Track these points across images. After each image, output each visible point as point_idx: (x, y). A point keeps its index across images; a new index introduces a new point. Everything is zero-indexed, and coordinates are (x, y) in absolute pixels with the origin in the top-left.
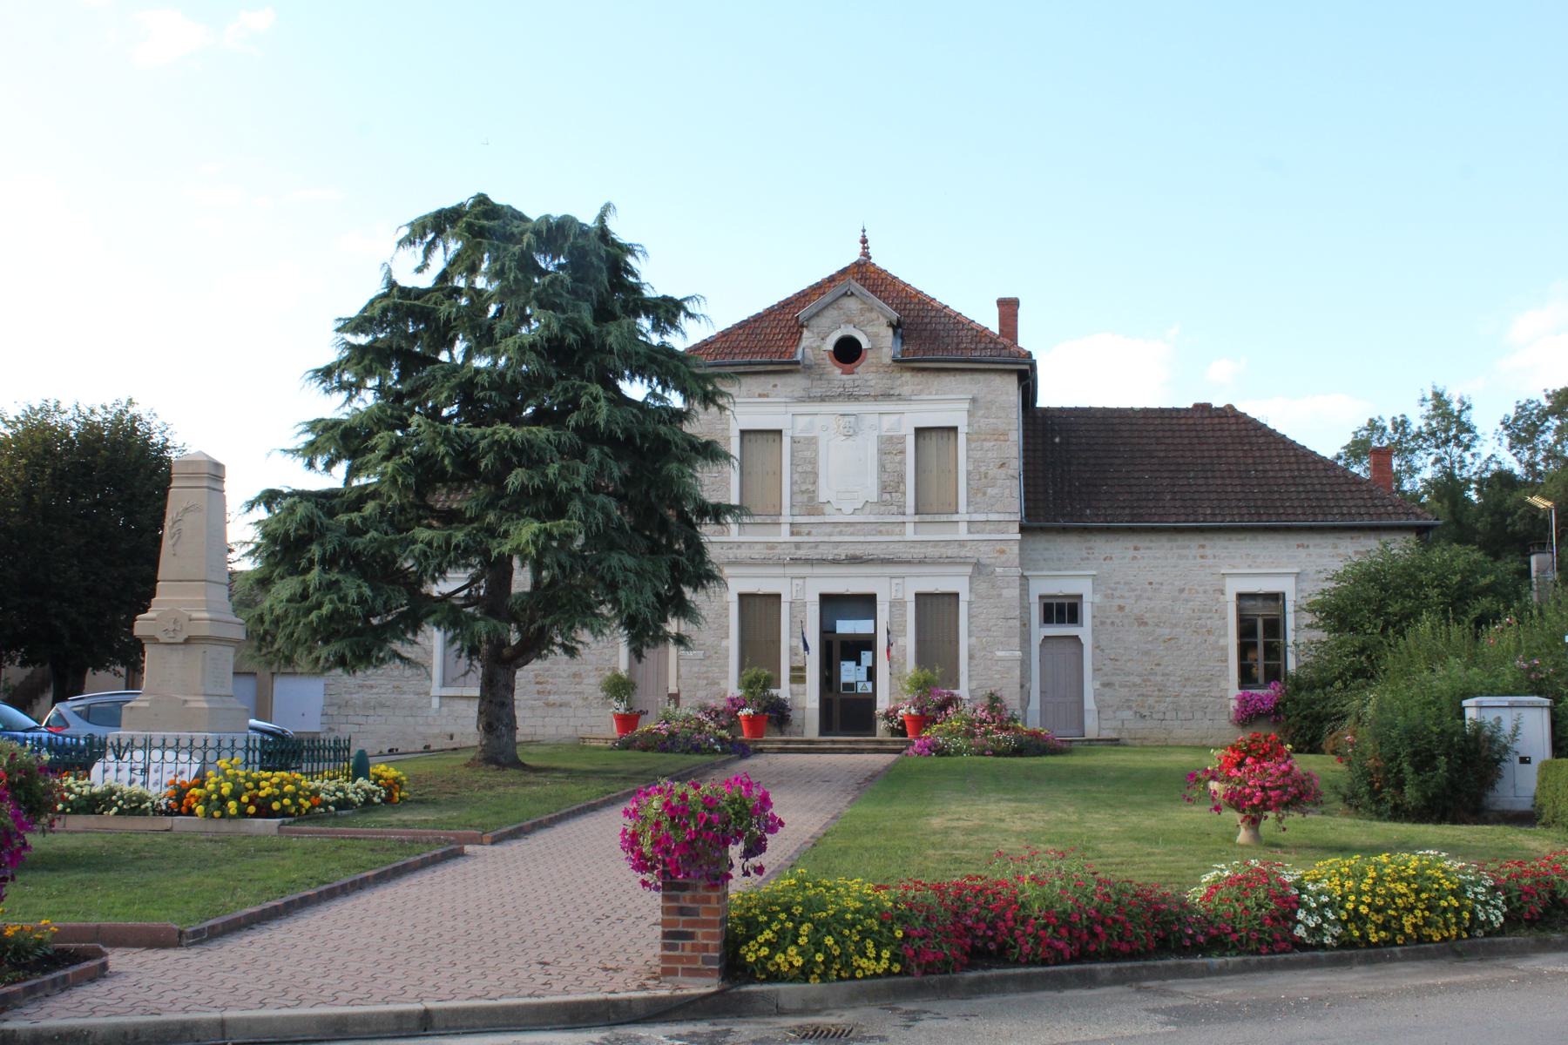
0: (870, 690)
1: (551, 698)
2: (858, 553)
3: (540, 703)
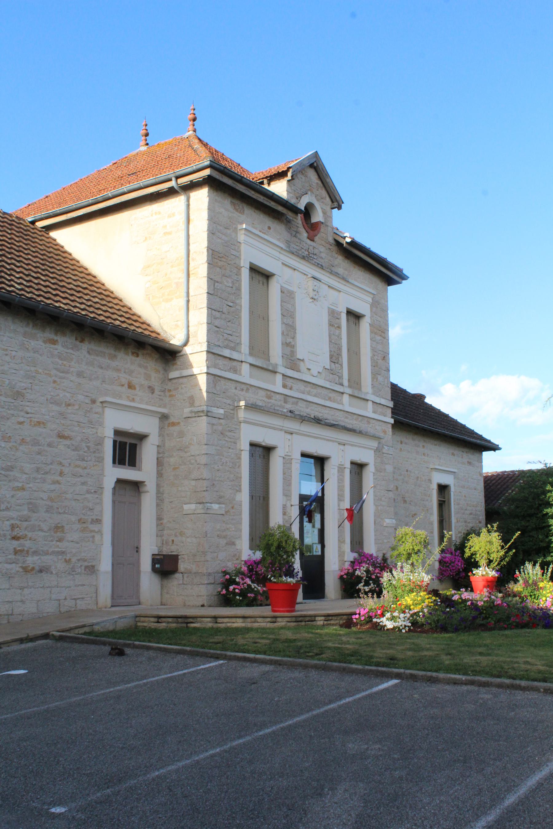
0: (320, 553)
1: (31, 560)
2: (319, 415)
3: (15, 568)
